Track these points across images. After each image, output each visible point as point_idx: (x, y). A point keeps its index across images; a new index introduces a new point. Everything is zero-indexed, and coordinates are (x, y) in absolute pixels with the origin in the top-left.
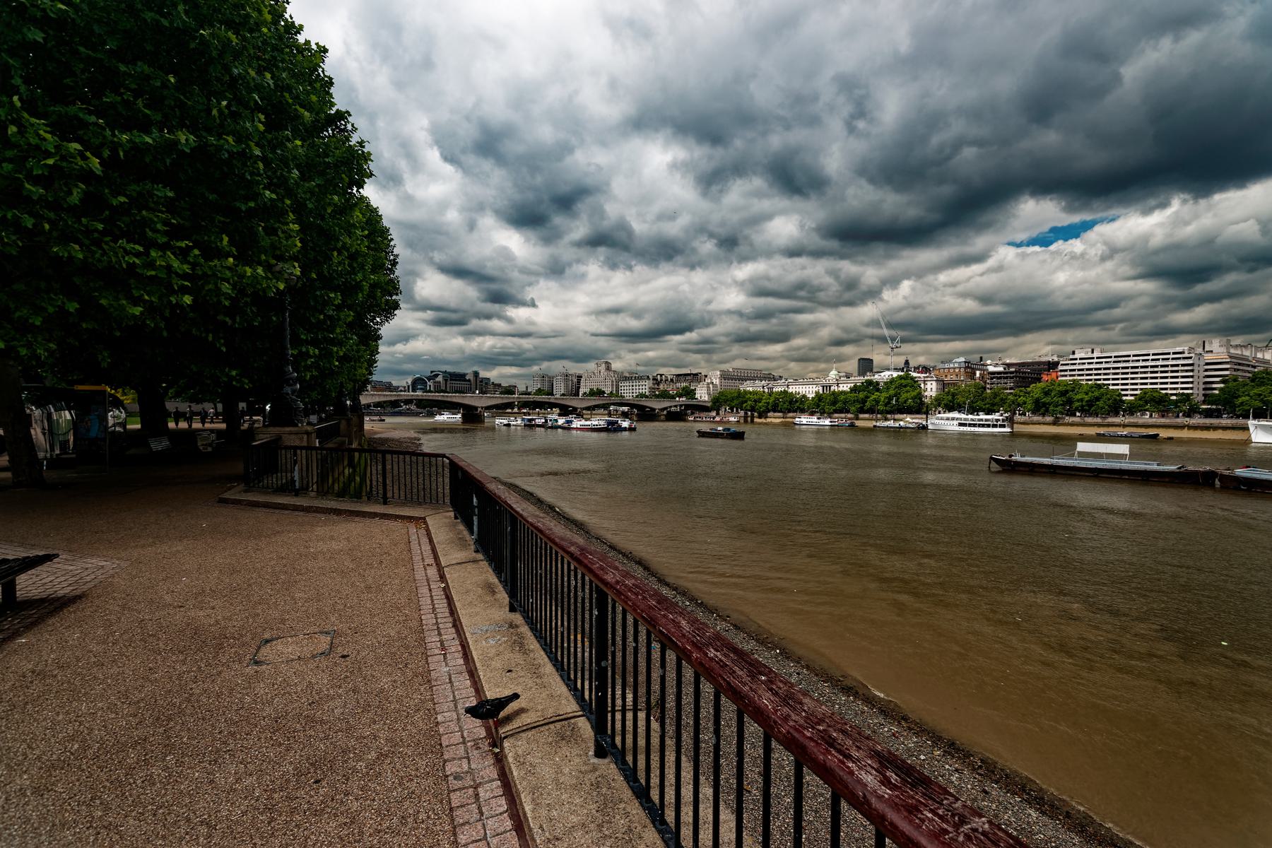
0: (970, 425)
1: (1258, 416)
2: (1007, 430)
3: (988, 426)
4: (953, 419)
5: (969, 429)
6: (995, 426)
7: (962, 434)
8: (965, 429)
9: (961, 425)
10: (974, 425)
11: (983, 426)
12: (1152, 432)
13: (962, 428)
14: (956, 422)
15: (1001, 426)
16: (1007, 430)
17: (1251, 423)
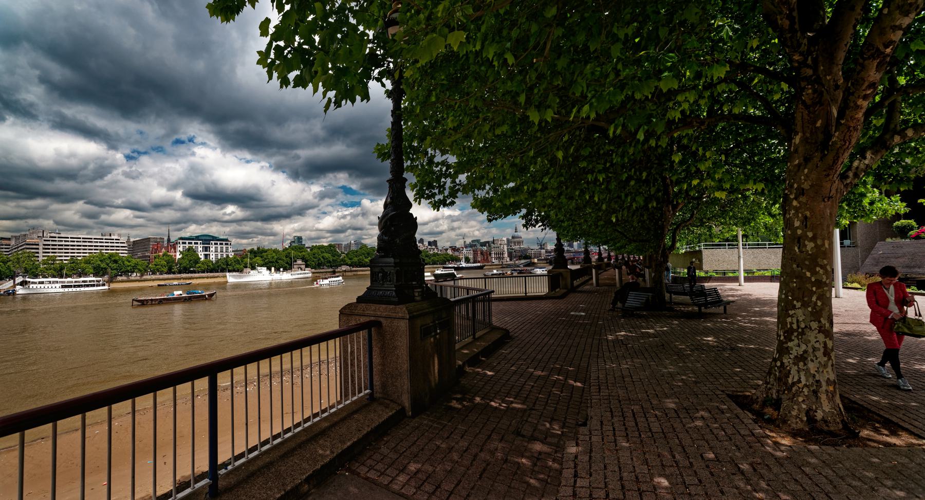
0: (75, 286)
1: (229, 271)
2: (106, 287)
3: (94, 285)
4: (54, 282)
5: (74, 289)
6: (98, 286)
7: (63, 294)
8: (70, 290)
9: (63, 287)
10: (79, 286)
11: (88, 286)
12: (188, 282)
13: (66, 290)
14: (58, 285)
15: (104, 285)
16: (106, 287)
17: (228, 274)
